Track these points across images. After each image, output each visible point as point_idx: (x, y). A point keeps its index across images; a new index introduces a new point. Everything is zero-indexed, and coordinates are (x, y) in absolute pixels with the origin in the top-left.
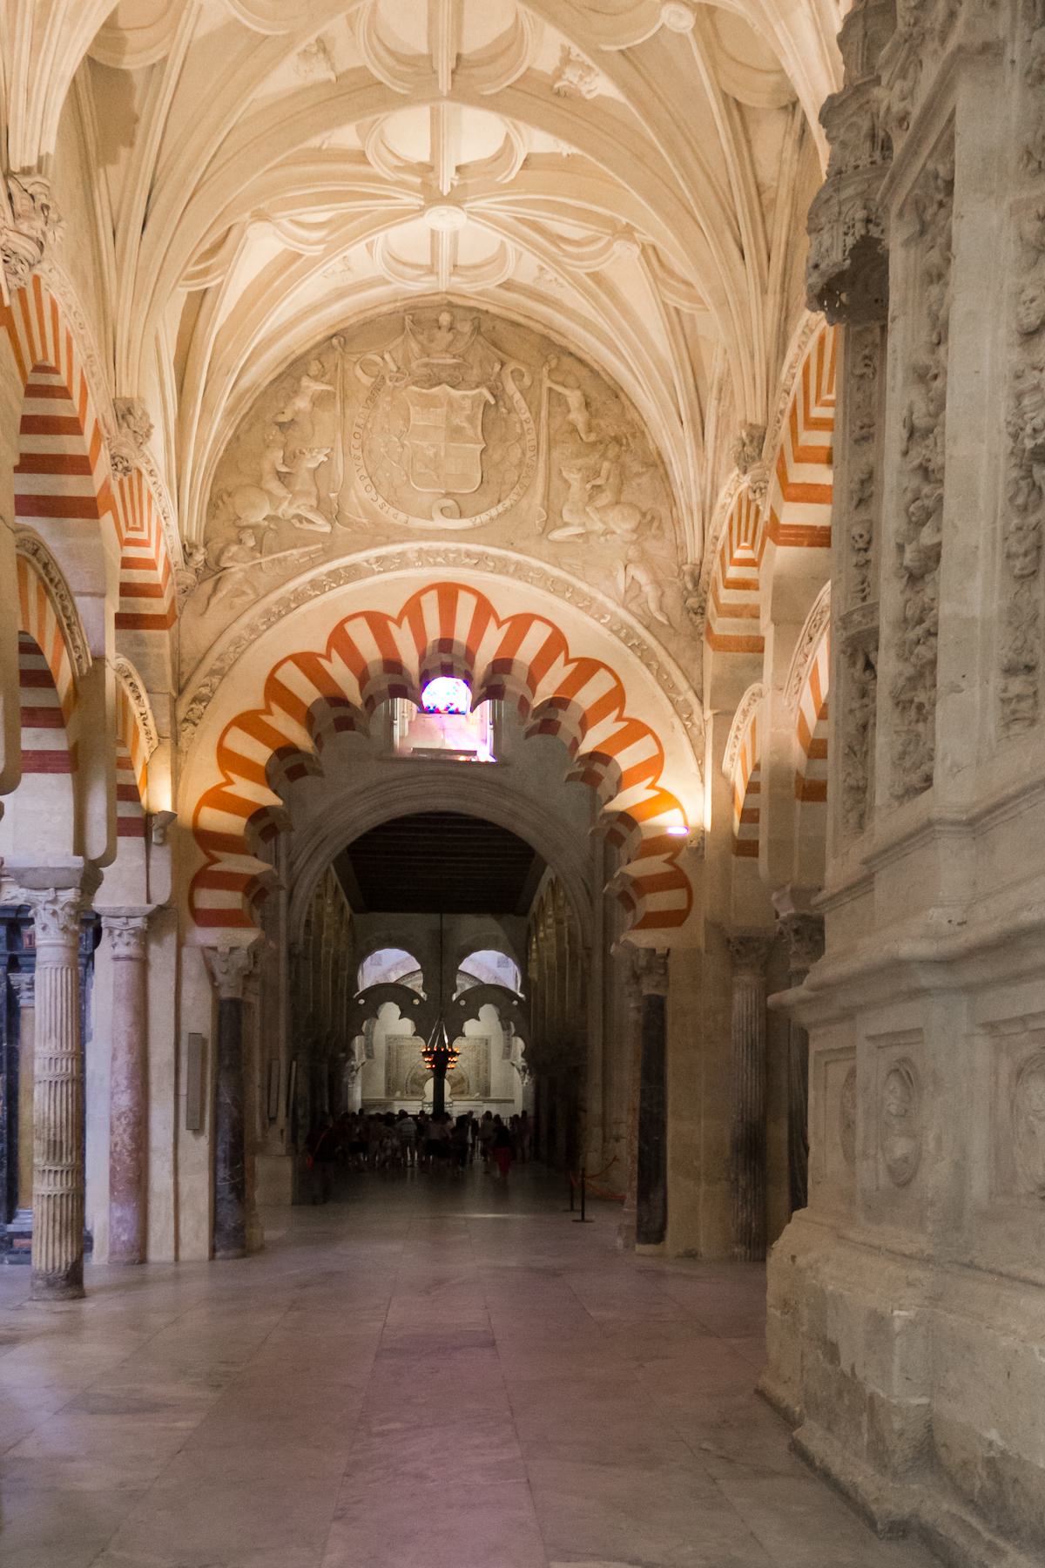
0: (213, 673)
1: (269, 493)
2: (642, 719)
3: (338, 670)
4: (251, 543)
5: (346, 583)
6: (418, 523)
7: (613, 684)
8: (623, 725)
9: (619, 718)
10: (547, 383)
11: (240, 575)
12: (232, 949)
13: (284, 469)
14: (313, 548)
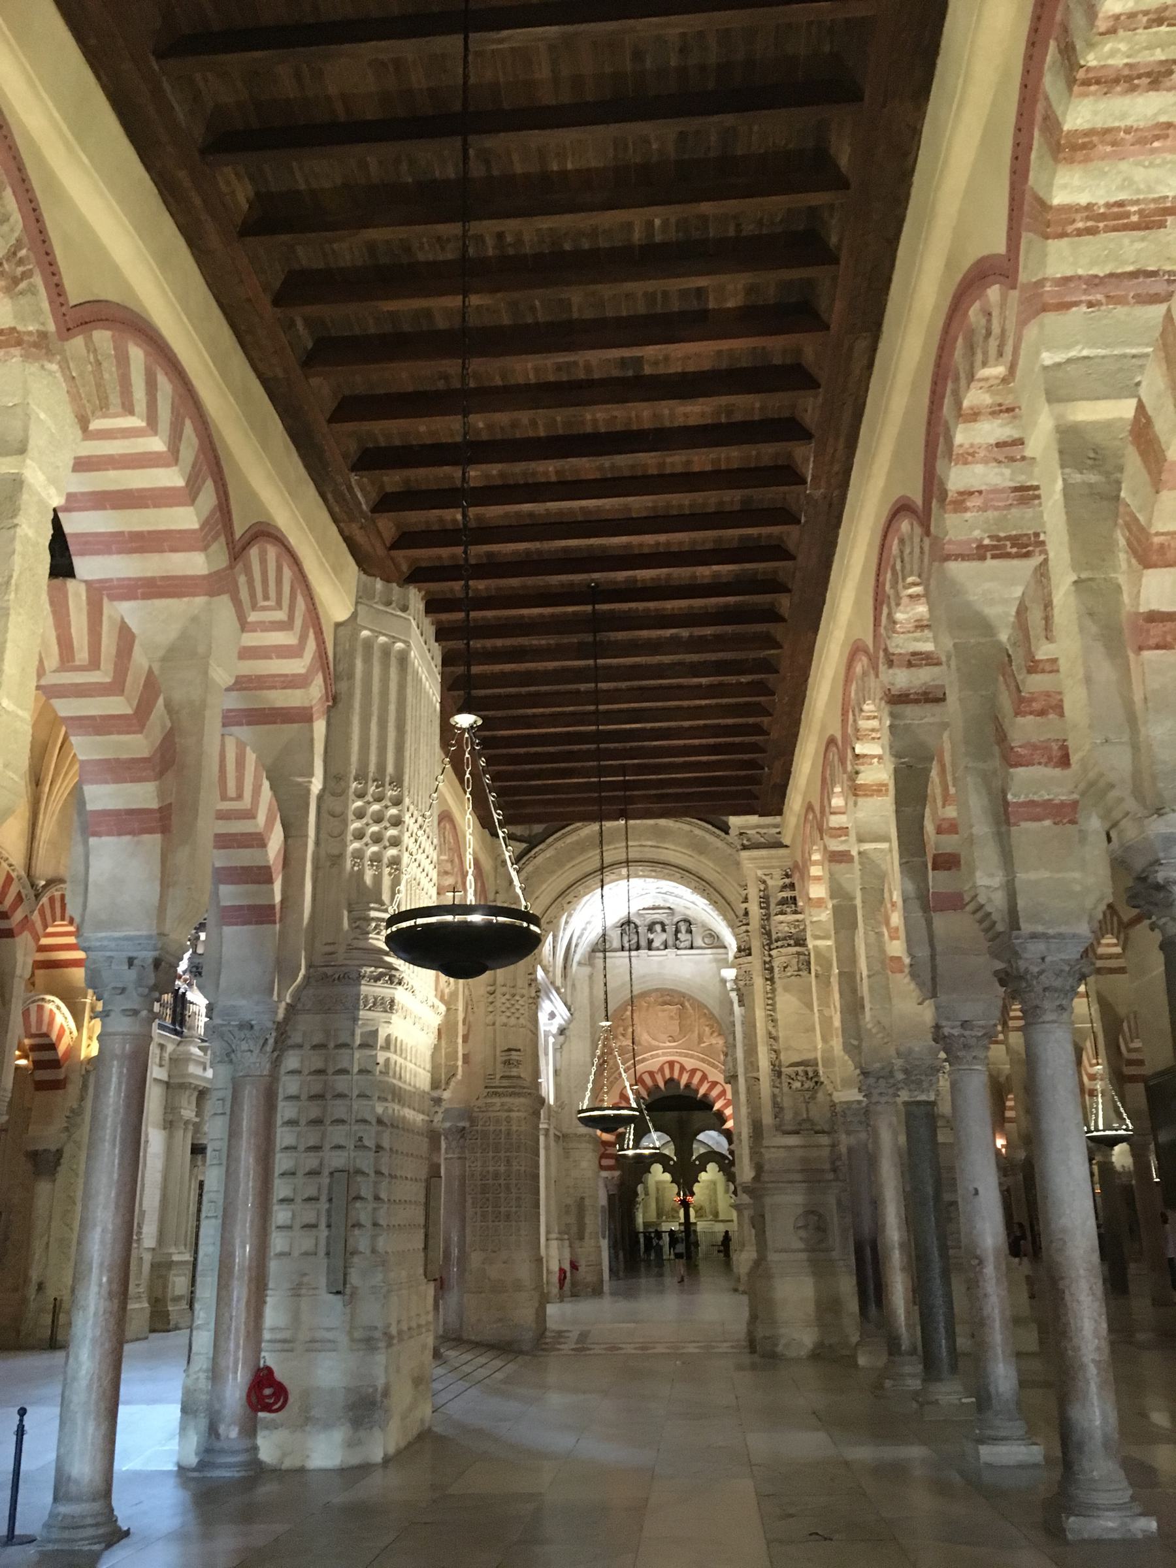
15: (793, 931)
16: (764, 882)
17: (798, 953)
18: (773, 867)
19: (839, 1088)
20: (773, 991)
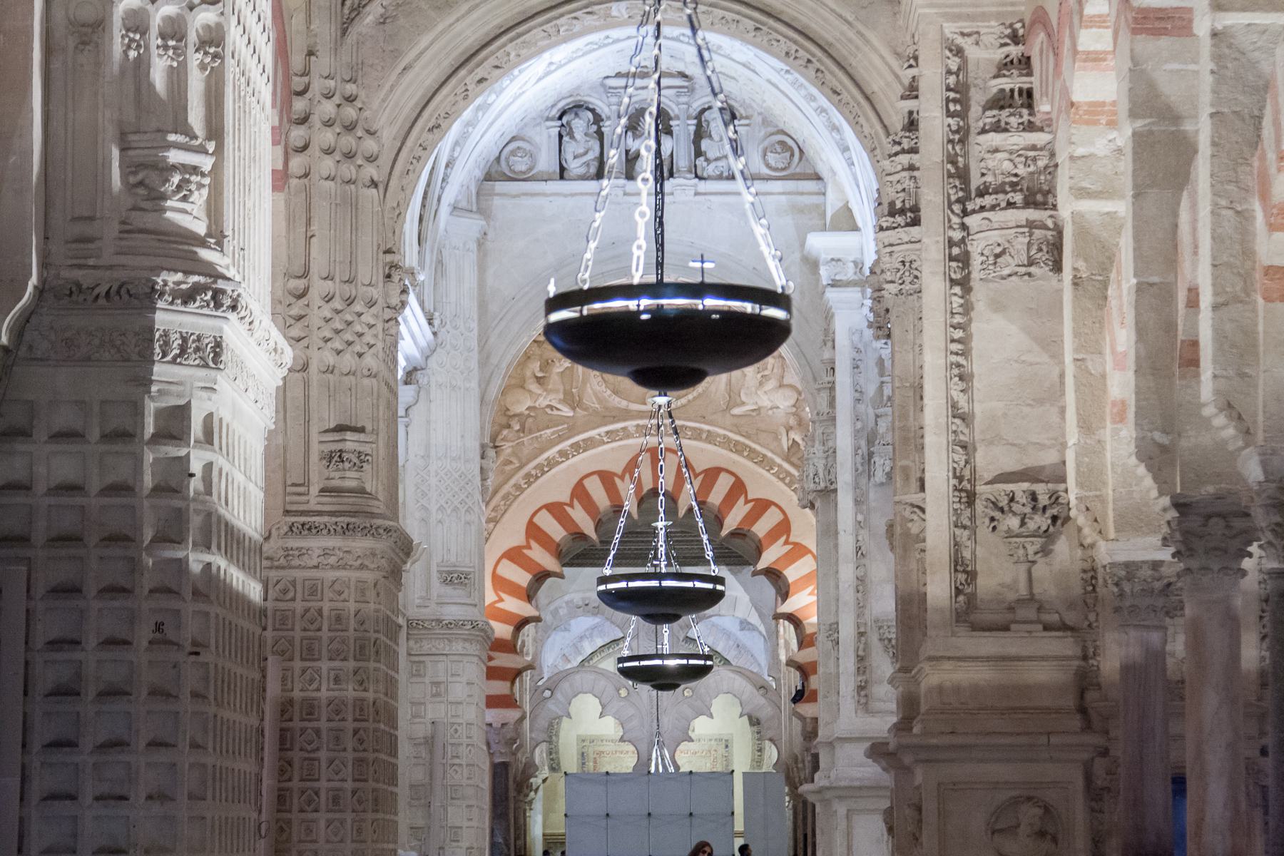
1: (530, 391)
2: (804, 543)
4: (517, 427)
5: (584, 451)
7: (781, 517)
8: (789, 547)
9: (786, 543)
11: (509, 451)
12: (503, 725)
13: (540, 375)
15: (1021, 170)
16: (959, 52)
17: (1031, 225)
18: (984, 17)
19: (1112, 535)
20: (967, 309)
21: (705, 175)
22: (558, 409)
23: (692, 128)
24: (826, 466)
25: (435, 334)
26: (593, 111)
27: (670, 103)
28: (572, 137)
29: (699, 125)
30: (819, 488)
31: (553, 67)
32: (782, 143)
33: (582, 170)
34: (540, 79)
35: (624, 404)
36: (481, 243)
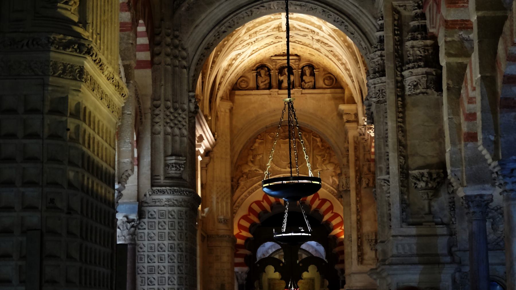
0: (236, 207)
1: (249, 166)
3: (265, 204)
4: (245, 177)
6: (283, 170)
10: (312, 137)
13: (252, 160)
14: (259, 177)
16: (398, 12)
19: (465, 184)
21: (305, 87)
22: (259, 171)
23: (300, 72)
24: (346, 182)
25: (215, 140)
26: (267, 67)
27: (293, 65)
28: (260, 76)
29: (302, 72)
30: (344, 190)
31: (254, 52)
32: (330, 77)
33: (264, 87)
34: (249, 56)
35: (279, 169)
36: (231, 110)
